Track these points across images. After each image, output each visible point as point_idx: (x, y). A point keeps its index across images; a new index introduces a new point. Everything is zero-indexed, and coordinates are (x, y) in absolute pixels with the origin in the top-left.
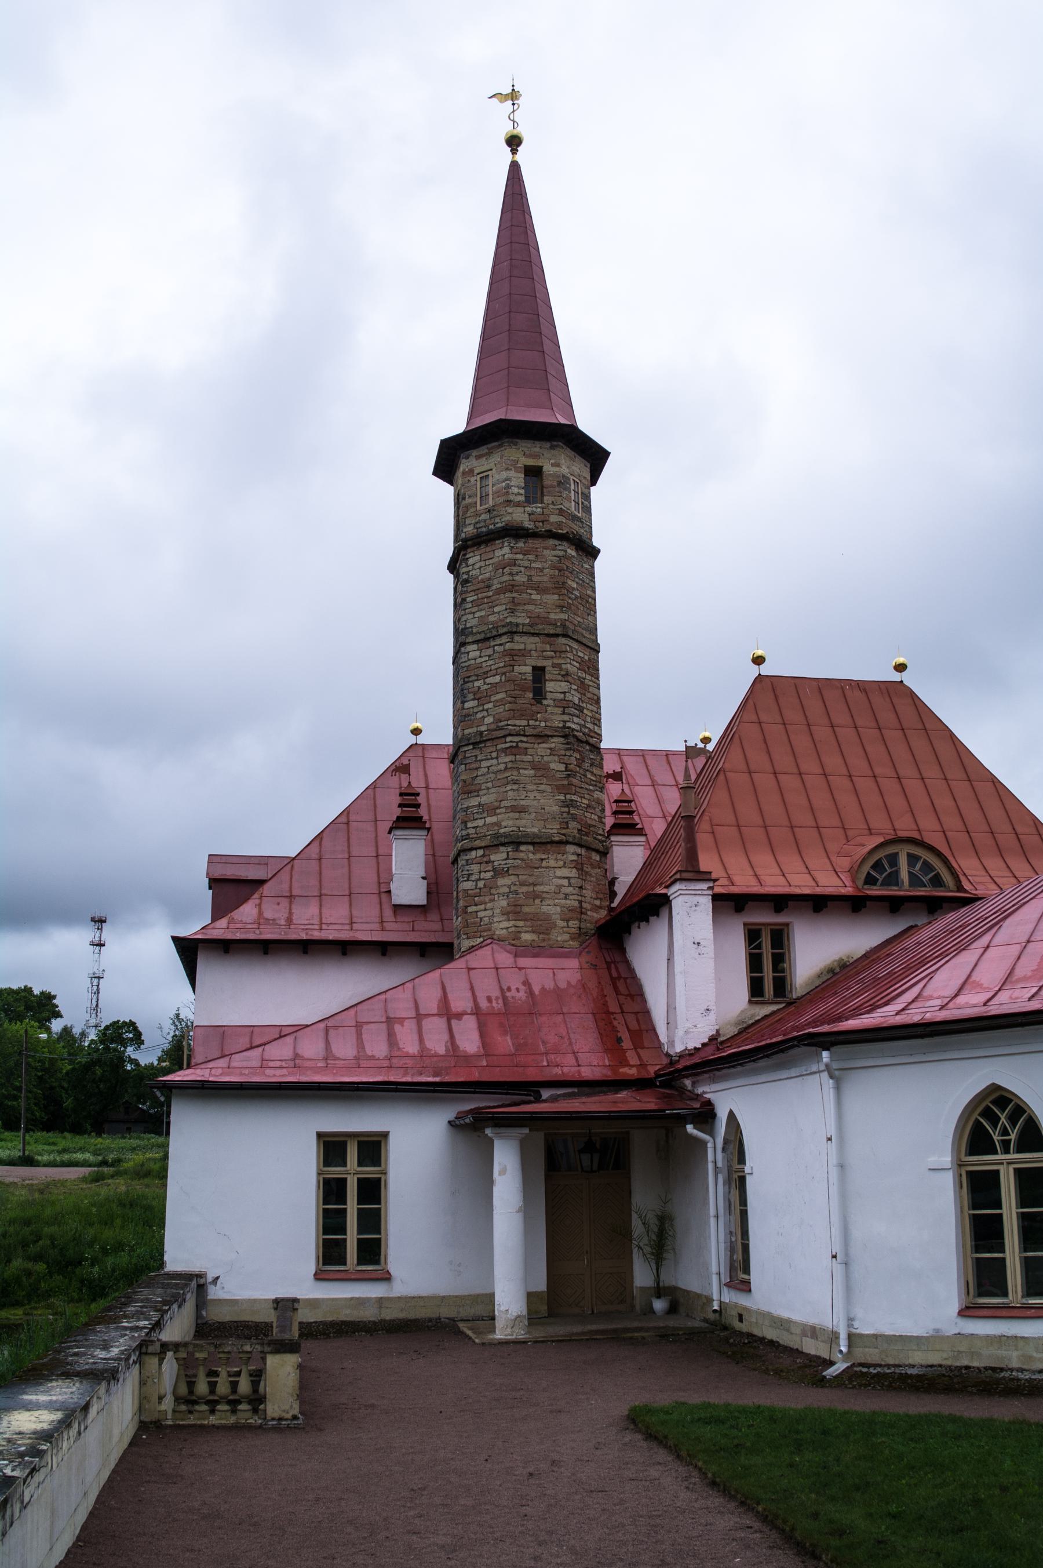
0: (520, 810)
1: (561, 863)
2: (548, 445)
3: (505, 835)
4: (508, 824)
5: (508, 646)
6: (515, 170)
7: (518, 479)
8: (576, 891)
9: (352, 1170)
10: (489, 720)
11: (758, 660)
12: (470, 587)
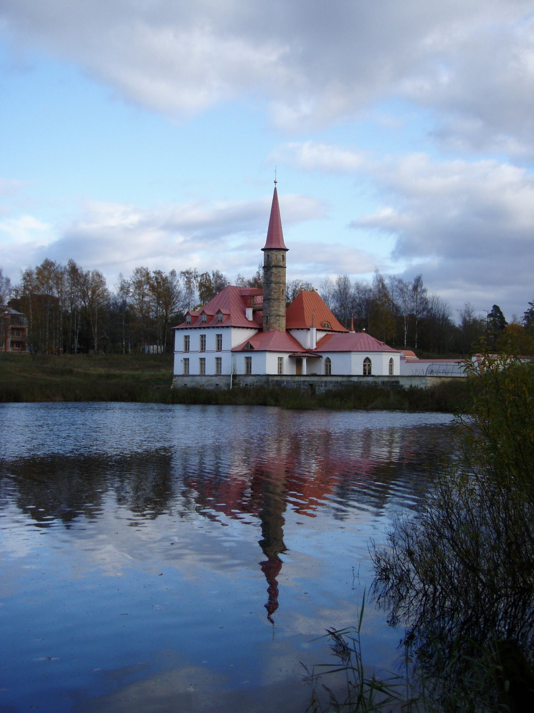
6: (275, 189)
7: (281, 258)
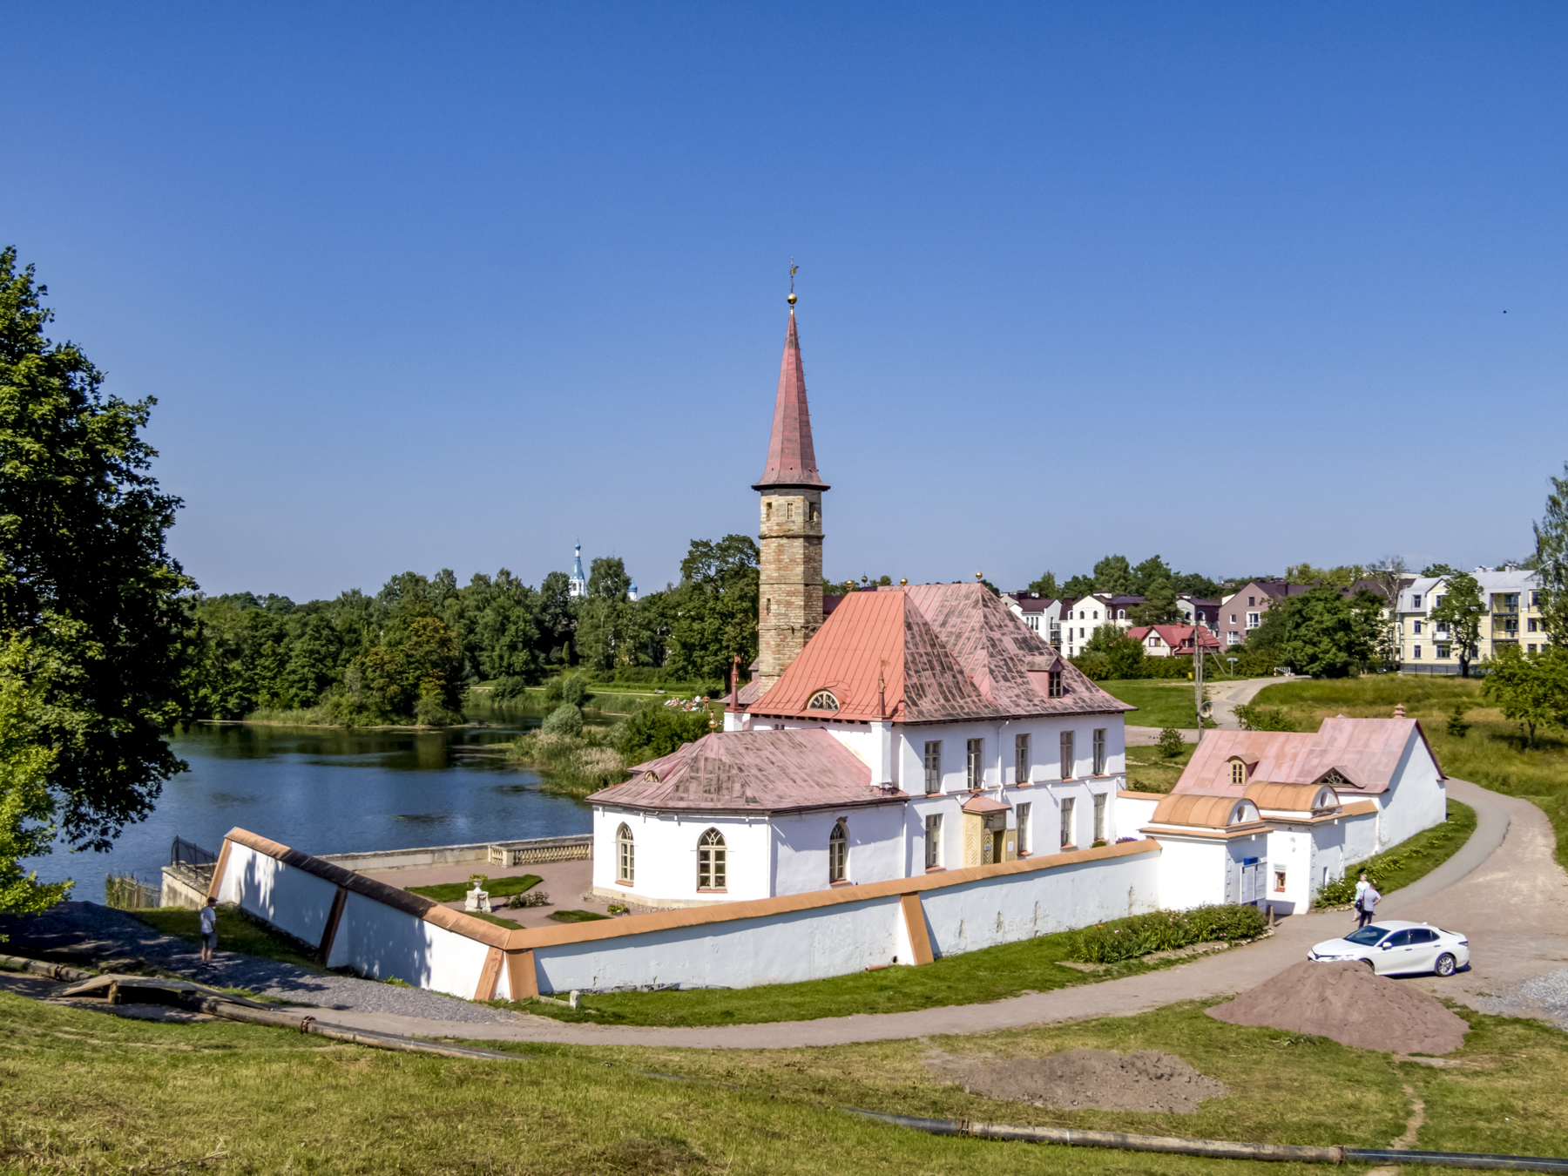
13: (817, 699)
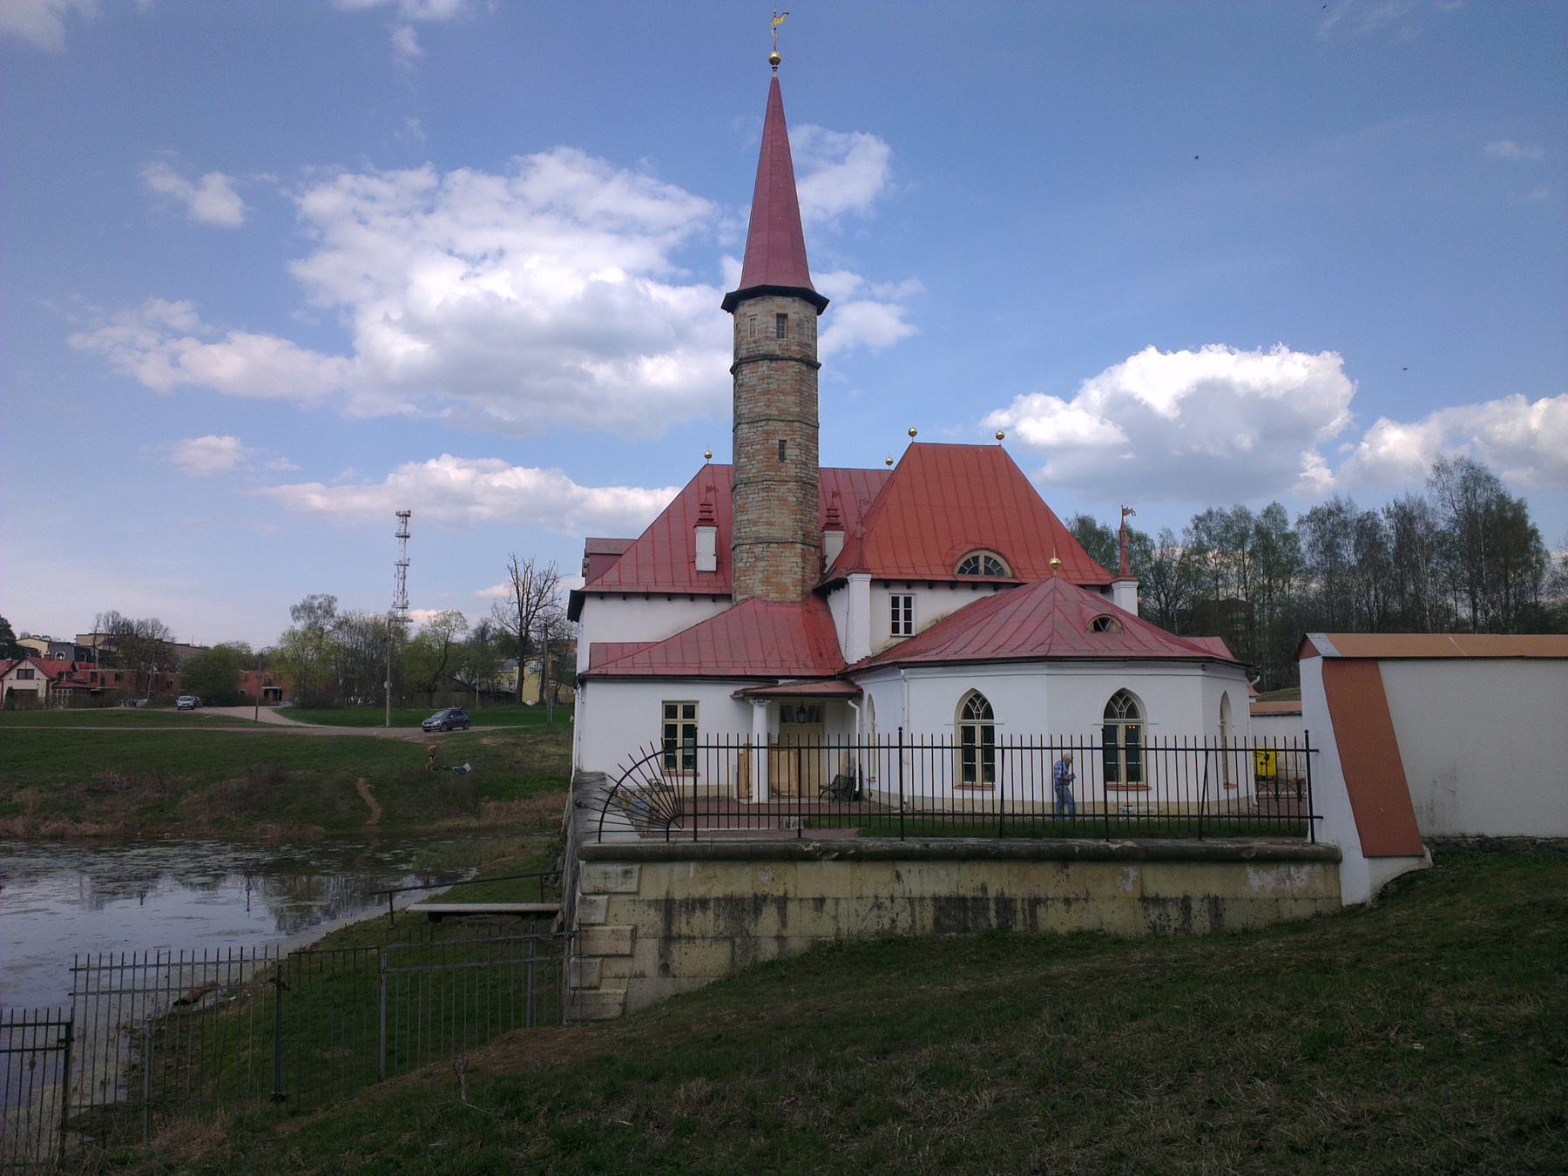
0: (770, 524)
1: (793, 554)
2: (790, 300)
3: (761, 538)
4: (763, 531)
5: (765, 428)
6: (775, 84)
7: (773, 323)
8: (801, 570)
9: (680, 721)
10: (754, 471)
11: (912, 434)
12: (743, 389)
13: (967, 563)
